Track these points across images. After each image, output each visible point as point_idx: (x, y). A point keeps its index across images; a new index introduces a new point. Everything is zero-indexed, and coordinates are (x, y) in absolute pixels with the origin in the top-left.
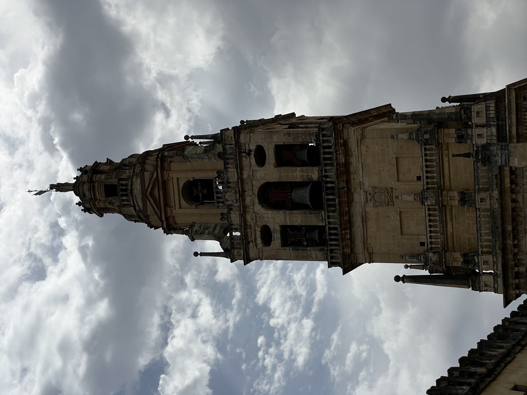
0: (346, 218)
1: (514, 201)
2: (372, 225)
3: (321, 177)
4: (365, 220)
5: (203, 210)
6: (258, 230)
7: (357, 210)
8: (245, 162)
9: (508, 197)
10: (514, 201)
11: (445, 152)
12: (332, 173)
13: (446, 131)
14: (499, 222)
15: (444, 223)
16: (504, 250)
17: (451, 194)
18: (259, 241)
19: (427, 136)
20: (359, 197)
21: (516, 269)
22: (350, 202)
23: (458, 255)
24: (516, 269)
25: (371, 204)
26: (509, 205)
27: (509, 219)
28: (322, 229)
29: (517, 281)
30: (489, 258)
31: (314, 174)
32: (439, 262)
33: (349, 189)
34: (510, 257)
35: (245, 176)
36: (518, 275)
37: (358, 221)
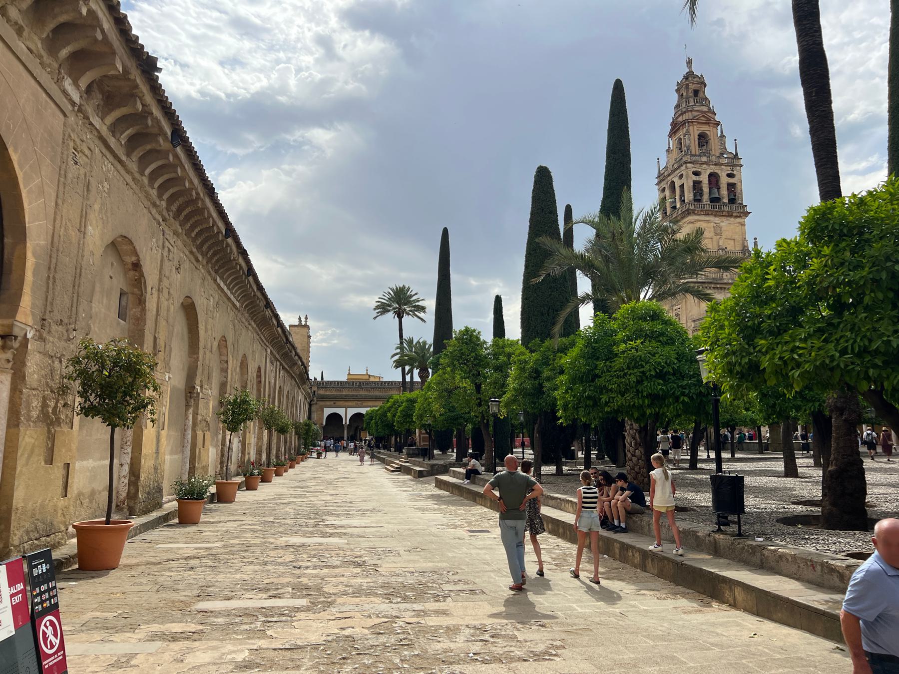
4: (708, 221)
6: (699, 170)
7: (711, 218)
8: (729, 168)
18: (695, 170)
20: (717, 220)
31: (726, 200)
33: (721, 216)
37: (707, 218)
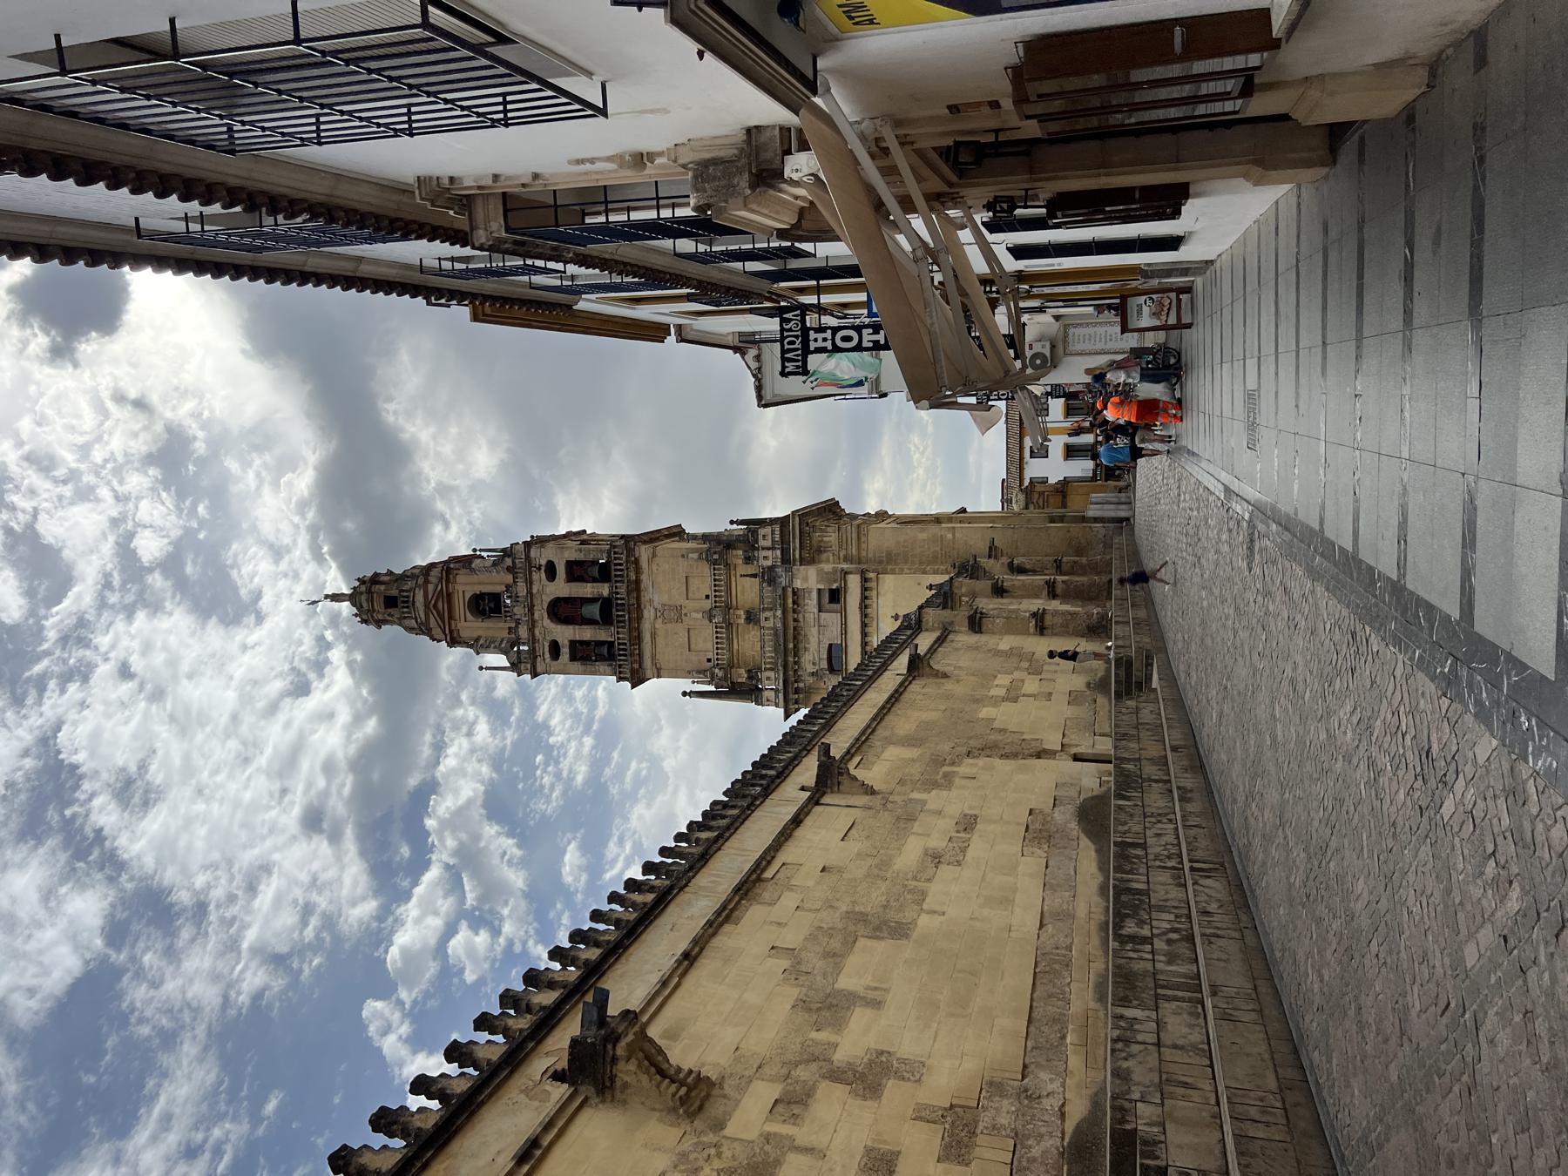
0: (636, 634)
1: (795, 620)
2: (660, 641)
3: (611, 593)
4: (654, 636)
5: (489, 624)
6: (547, 644)
7: (646, 626)
8: (535, 576)
9: (790, 616)
10: (795, 620)
11: (733, 572)
12: (622, 589)
13: (734, 552)
14: (782, 640)
15: (730, 640)
16: (785, 666)
17: (738, 612)
18: (547, 655)
19: (716, 557)
20: (648, 614)
22: (640, 618)
23: (742, 671)
25: (660, 620)
26: (791, 624)
27: (790, 636)
28: (611, 644)
30: (772, 674)
31: (604, 590)
32: (725, 678)
34: (791, 673)
35: (535, 591)
36: (797, 691)
37: (647, 637)
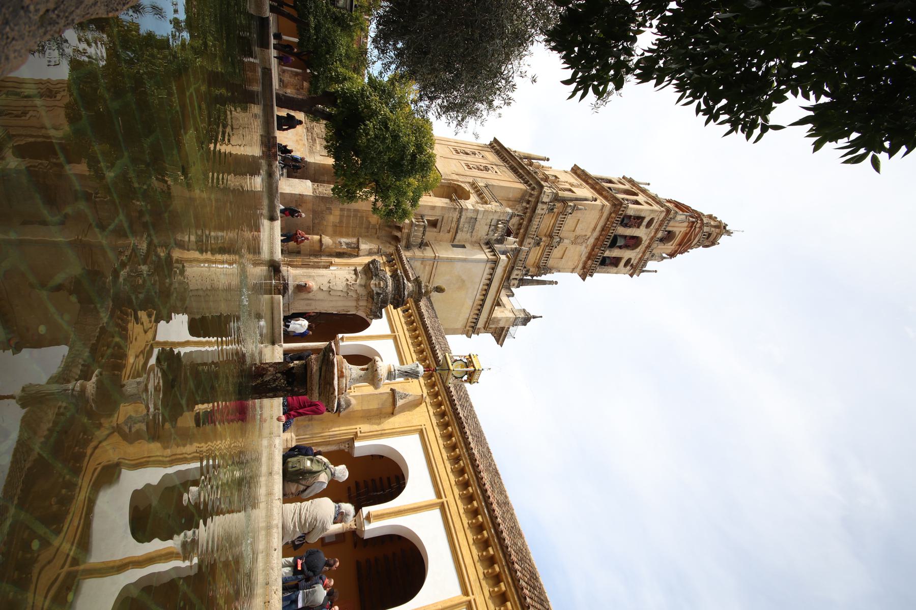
2: (592, 226)
6: (652, 227)
11: (537, 261)
20: (591, 241)
21: (528, 206)
24: (528, 206)
29: (530, 199)
36: (528, 202)
